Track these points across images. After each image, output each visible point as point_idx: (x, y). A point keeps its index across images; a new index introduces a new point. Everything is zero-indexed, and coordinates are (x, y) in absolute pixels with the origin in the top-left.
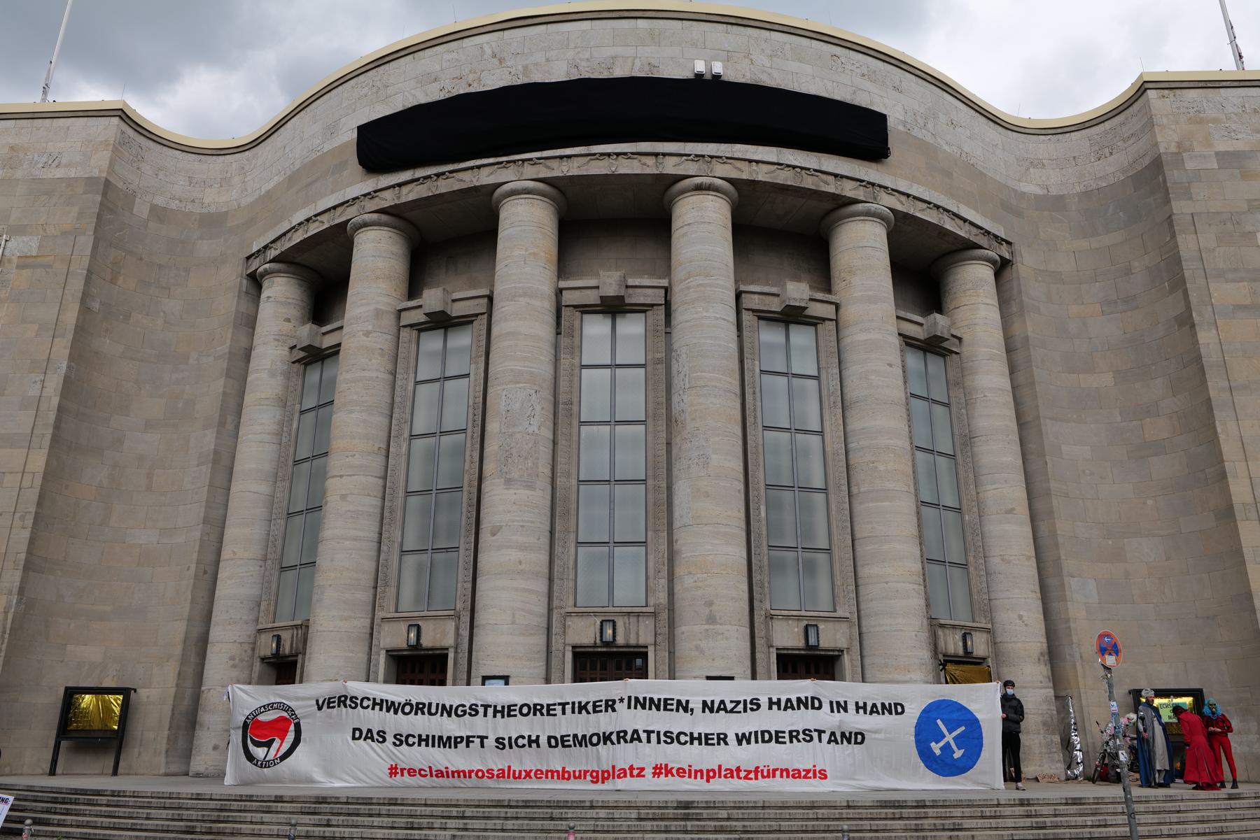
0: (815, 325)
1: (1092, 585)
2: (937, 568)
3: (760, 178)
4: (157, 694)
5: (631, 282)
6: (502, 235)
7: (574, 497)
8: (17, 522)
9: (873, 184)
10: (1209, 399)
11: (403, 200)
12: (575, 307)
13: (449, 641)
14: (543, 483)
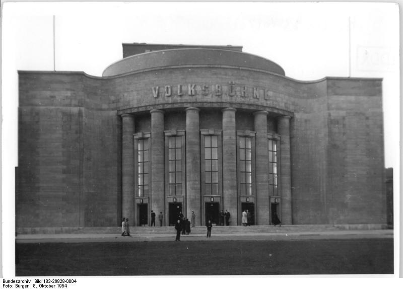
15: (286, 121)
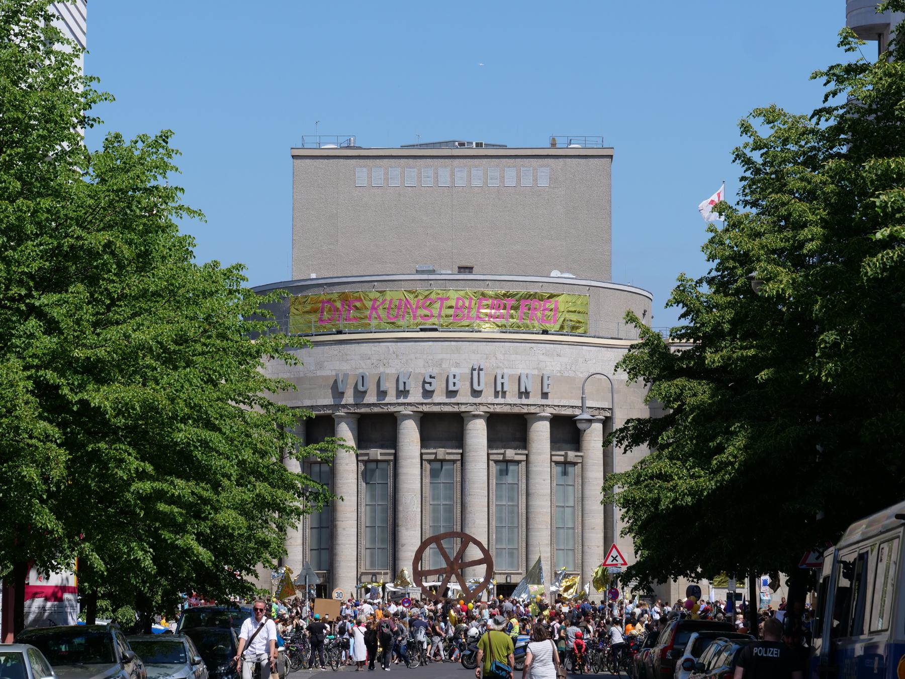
2: (561, 552)
15: (598, 427)
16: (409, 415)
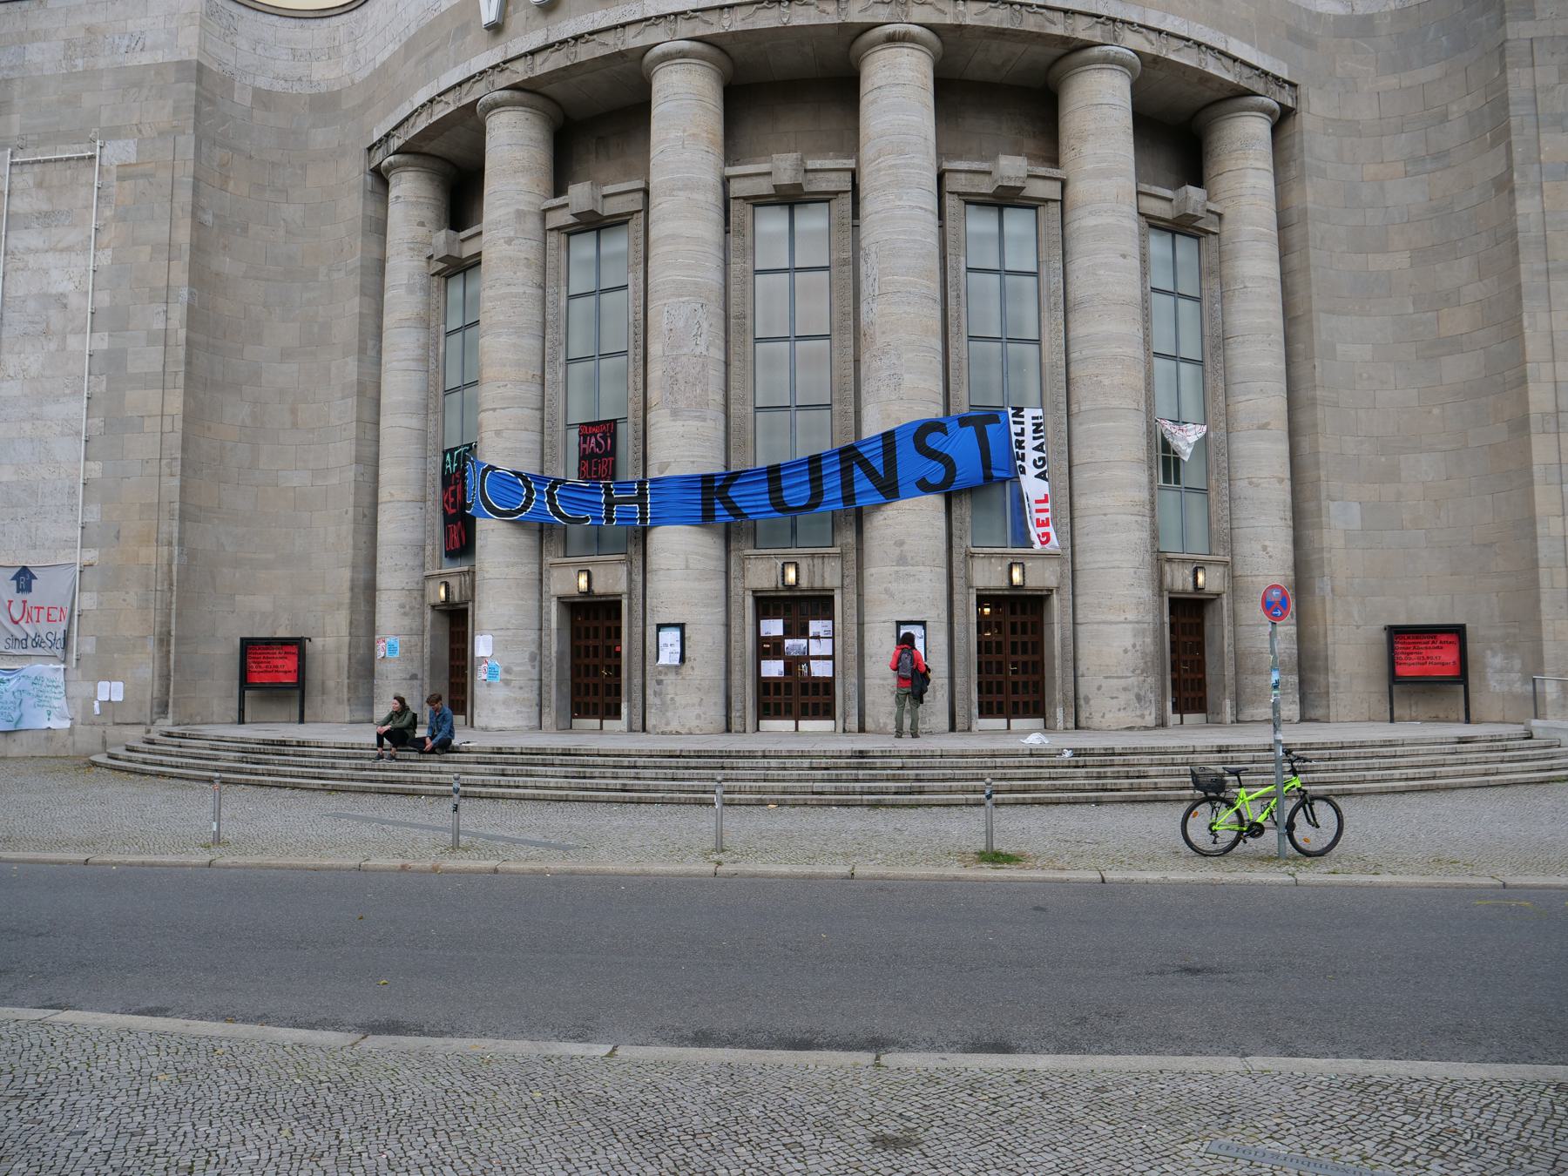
0: (1036, 208)
1: (1356, 508)
3: (968, 21)
4: (330, 644)
5: (811, 164)
6: (656, 111)
7: (750, 427)
8: (165, 470)
9: (1114, 20)
10: (1519, 286)
11: (539, 71)
12: (745, 198)
13: (622, 587)
14: (715, 413)
16: (682, 54)
